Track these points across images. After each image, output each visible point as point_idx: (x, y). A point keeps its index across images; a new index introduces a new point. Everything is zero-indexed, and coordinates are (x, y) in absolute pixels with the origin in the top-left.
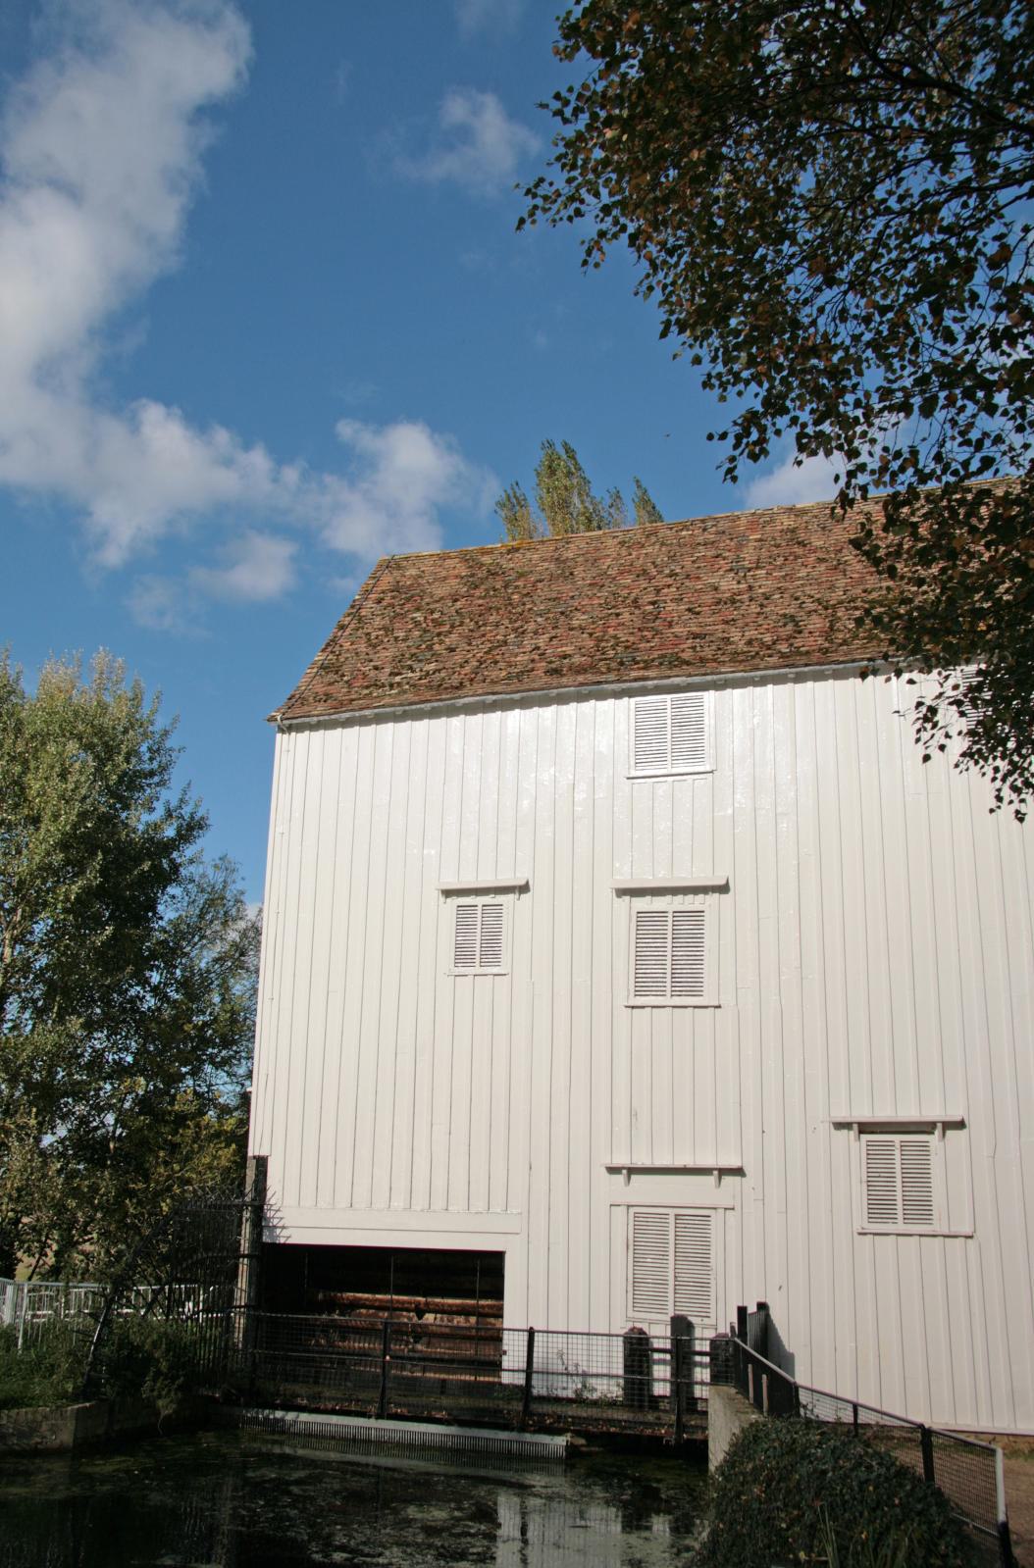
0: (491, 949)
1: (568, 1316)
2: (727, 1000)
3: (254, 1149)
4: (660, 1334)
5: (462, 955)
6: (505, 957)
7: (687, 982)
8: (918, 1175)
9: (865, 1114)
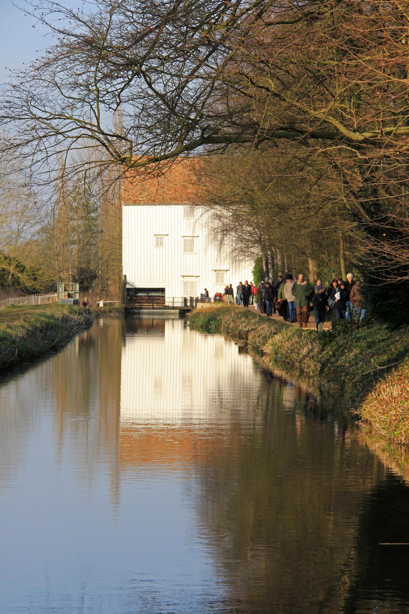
0: (162, 244)
1: (174, 296)
2: (198, 253)
3: (124, 273)
4: (188, 299)
5: (157, 245)
6: (164, 245)
7: (191, 250)
8: (222, 278)
9: (216, 269)
